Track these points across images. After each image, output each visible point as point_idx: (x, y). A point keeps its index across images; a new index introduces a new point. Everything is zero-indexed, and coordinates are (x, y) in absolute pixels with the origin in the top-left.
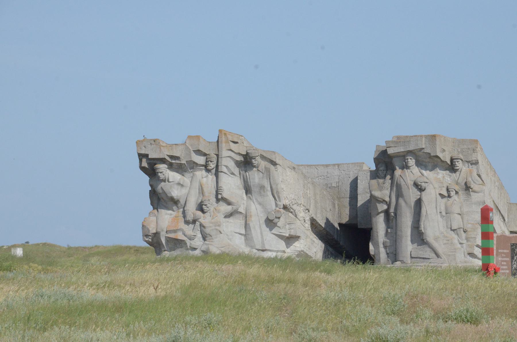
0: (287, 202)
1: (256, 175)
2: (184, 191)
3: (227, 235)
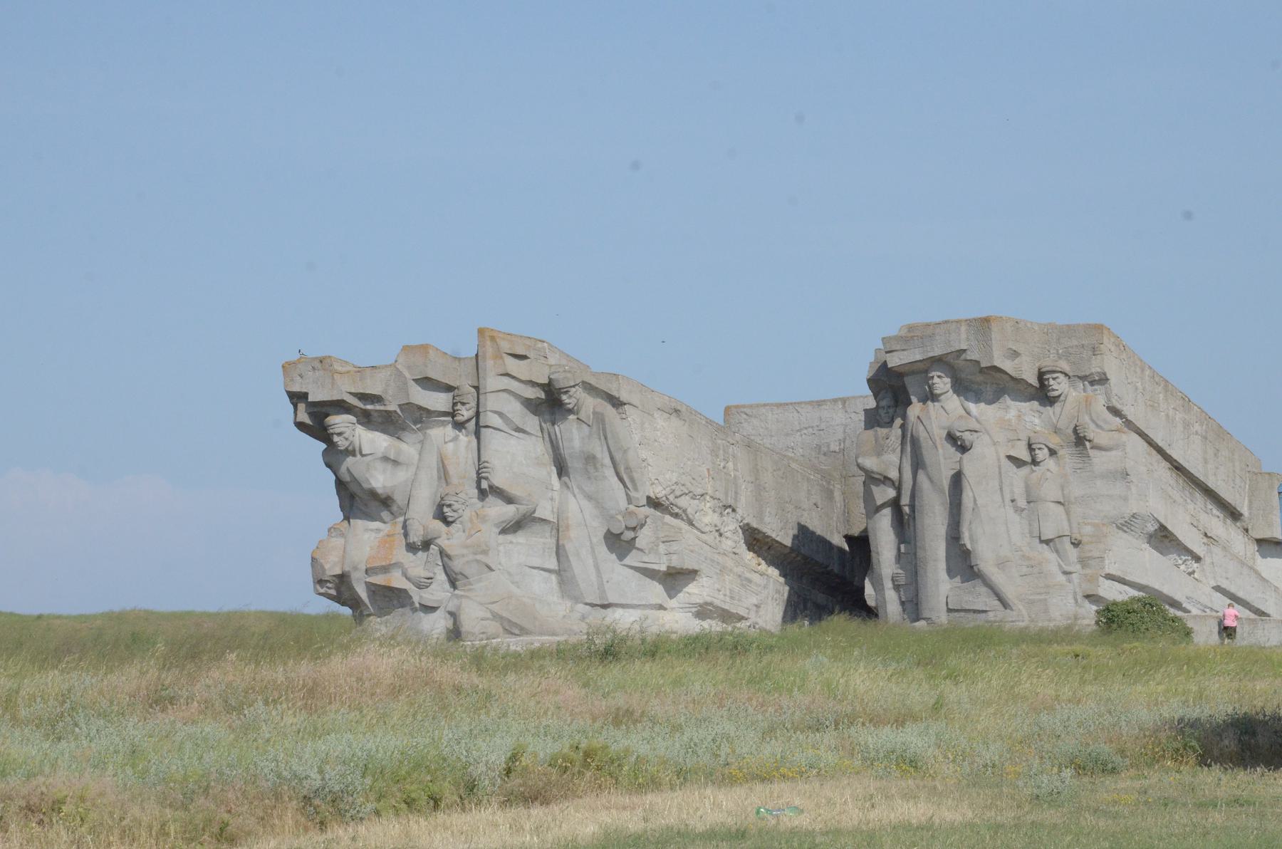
0: (658, 492)
1: (574, 431)
2: (402, 475)
3: (509, 573)
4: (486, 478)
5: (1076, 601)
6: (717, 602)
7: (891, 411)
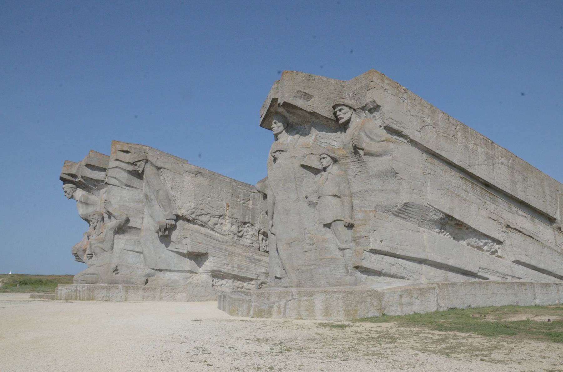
0: (180, 213)
2: (90, 210)
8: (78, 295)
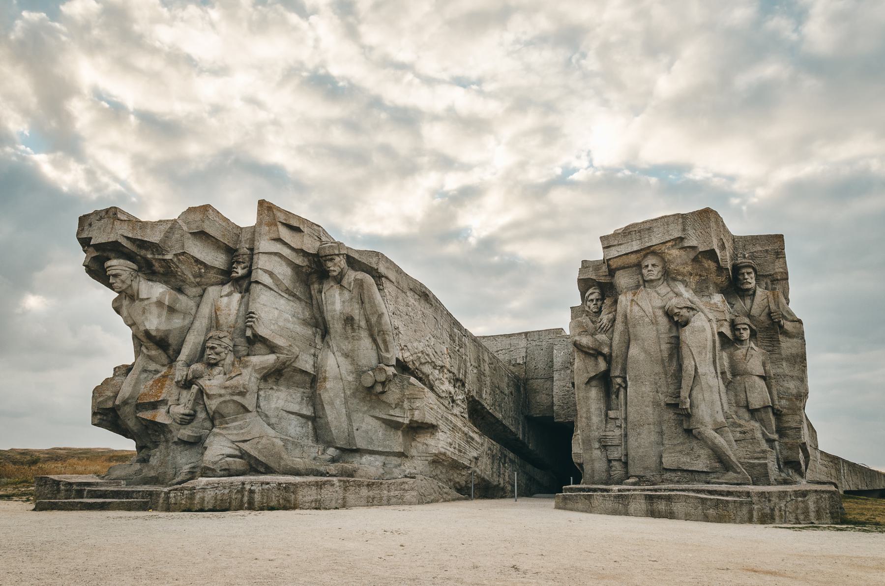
0: (407, 356)
1: (337, 296)
3: (266, 416)
4: (251, 327)
5: (779, 465)
6: (449, 453)
7: (599, 303)
8: (246, 499)
